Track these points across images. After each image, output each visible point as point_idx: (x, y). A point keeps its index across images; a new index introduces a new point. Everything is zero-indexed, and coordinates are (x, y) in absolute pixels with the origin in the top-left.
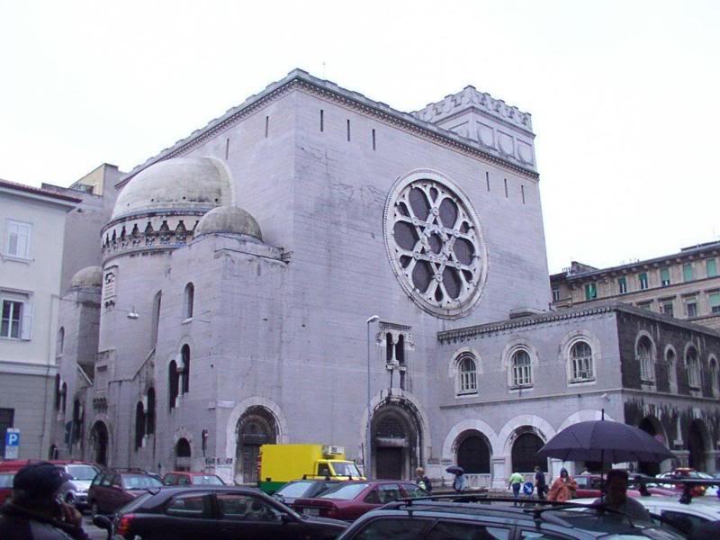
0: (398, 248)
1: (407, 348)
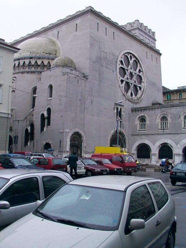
1: (122, 113)
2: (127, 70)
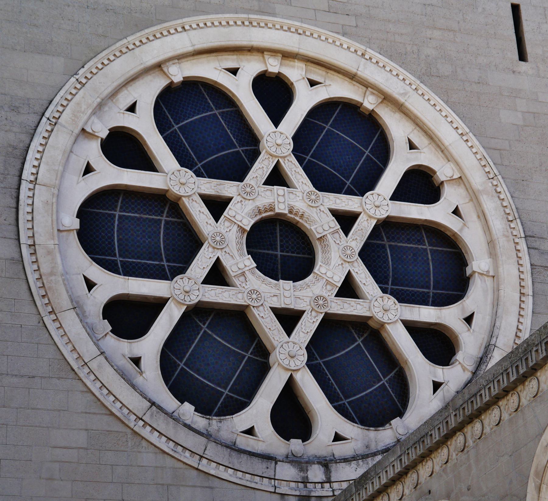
0: (96, 272)
2: (217, 206)
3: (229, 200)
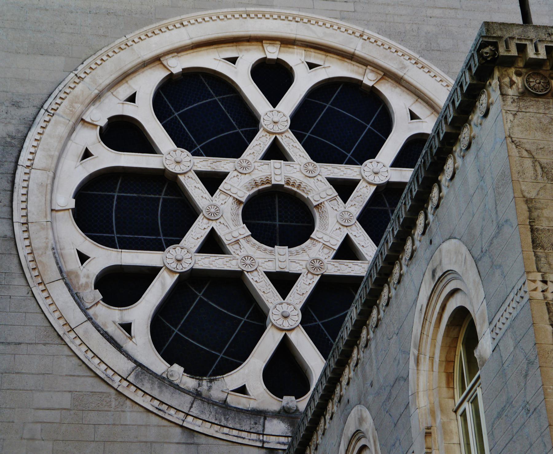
2: (212, 181)
3: (224, 175)
